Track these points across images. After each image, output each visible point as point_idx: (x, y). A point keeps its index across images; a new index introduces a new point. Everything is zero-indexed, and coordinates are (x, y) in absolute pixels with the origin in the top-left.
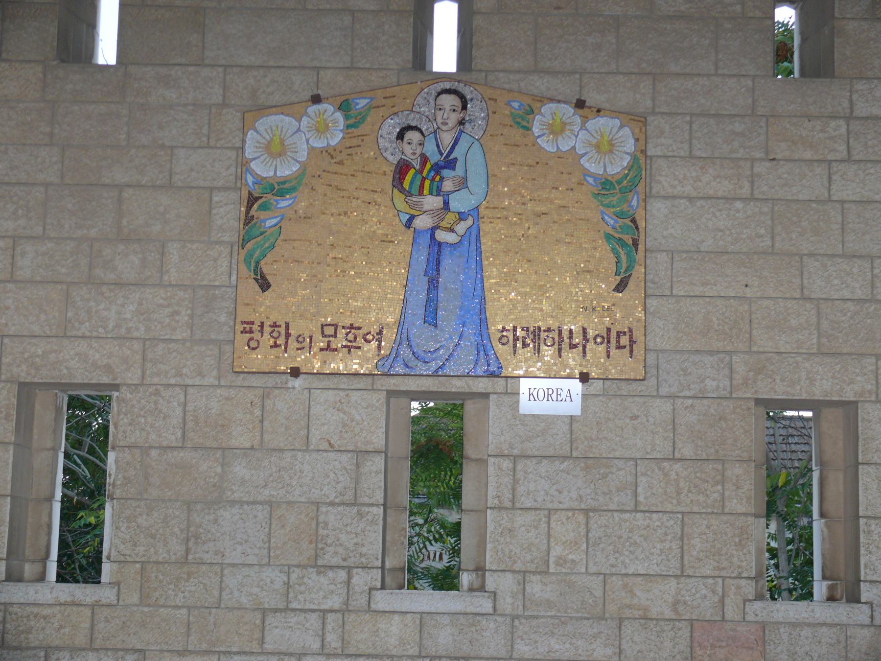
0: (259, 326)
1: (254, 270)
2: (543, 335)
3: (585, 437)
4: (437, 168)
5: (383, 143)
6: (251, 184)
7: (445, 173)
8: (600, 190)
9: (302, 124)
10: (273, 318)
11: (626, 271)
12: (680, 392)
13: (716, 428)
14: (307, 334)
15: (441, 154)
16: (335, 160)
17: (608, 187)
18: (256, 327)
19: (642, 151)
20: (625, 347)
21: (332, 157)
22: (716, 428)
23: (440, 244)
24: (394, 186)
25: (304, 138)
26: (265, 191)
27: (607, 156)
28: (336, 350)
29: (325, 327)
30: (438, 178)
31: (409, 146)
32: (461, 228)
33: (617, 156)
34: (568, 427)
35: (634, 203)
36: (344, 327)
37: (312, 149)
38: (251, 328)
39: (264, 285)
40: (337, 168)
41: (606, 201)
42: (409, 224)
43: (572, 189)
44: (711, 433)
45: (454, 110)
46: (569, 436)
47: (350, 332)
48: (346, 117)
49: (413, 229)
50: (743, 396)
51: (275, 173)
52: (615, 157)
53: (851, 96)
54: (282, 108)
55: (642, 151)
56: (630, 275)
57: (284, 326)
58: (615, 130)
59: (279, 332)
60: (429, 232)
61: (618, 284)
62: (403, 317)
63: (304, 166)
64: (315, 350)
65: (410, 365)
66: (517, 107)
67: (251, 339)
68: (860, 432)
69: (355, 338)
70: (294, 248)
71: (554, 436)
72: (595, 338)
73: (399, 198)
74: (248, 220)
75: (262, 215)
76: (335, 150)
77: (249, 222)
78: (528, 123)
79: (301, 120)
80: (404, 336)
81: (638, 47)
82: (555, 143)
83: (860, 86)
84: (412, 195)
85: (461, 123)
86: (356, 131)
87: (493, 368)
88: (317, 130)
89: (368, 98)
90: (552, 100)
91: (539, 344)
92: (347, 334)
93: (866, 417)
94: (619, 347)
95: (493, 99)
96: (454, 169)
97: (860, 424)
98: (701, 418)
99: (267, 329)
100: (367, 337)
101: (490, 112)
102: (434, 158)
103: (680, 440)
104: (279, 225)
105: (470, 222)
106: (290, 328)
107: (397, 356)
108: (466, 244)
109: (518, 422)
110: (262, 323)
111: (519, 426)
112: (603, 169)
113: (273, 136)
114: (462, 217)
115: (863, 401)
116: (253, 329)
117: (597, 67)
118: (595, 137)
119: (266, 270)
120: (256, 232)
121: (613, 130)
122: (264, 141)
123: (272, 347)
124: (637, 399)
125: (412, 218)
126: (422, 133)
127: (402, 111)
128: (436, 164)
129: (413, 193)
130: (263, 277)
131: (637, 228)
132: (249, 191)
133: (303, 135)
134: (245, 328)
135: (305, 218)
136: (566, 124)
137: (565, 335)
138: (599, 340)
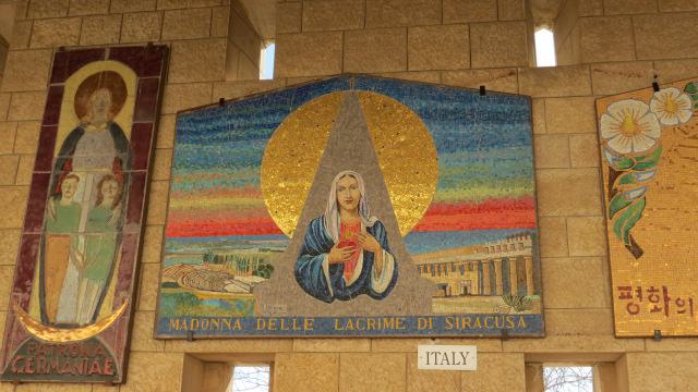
14: (686, 298)
18: (634, 294)
37: (664, 127)
39: (637, 252)
54: (629, 94)
57: (661, 290)
59: (657, 296)
63: (659, 142)
74: (612, 193)
75: (625, 187)
99: (645, 294)
120: (621, 203)
130: (634, 244)
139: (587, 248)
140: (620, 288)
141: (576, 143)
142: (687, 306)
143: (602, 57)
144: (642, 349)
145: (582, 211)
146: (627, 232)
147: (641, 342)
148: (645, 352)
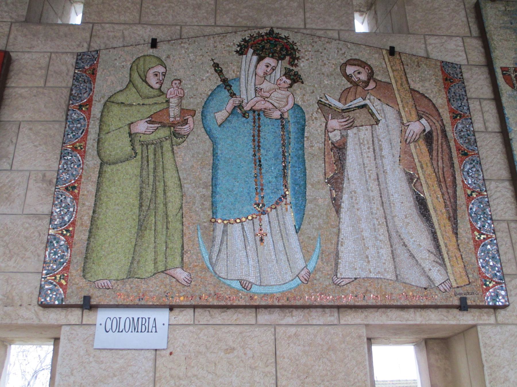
3: (172, 376)
12: (282, 320)
13: (325, 360)
22: (325, 360)
34: (151, 364)
44: (320, 366)
46: (151, 374)
50: (353, 323)
53: (426, 47)
68: (484, 359)
71: (135, 375)
81: (234, 7)
83: (431, 40)
93: (488, 342)
97: (483, 350)
98: (307, 348)
103: (283, 375)
109: (91, 359)
111: (93, 364)
115: (482, 324)
117: (197, 21)
124: (232, 328)
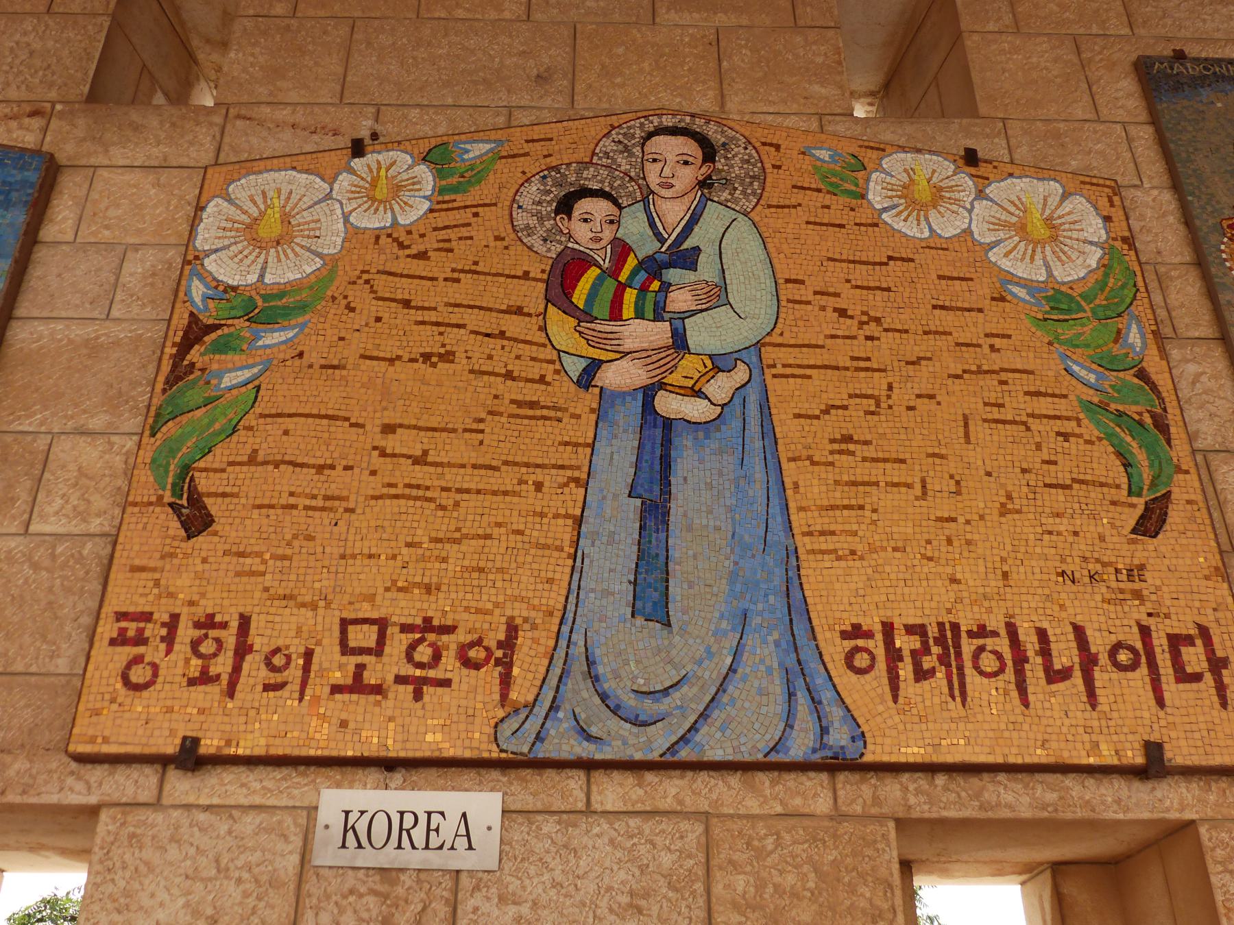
0: (164, 625)
1: (174, 485)
2: (968, 646)
4: (653, 267)
5: (521, 219)
6: (198, 299)
7: (673, 275)
8: (1046, 313)
9: (336, 186)
10: (207, 606)
11: (1153, 485)
14: (297, 648)
15: (662, 241)
16: (407, 252)
17: (1064, 306)
19: (1125, 240)
20: (1197, 677)
21: (401, 246)
23: (668, 423)
24: (548, 301)
25: (339, 212)
26: (233, 313)
27: (1048, 248)
28: (378, 690)
29: (351, 628)
30: (655, 285)
31: (584, 224)
32: (721, 387)
33: (1072, 248)
35: (1134, 337)
36: (406, 628)
37: (353, 233)
38: (141, 631)
40: (418, 267)
41: (1067, 332)
42: (587, 378)
43: (980, 310)
45: (686, 163)
47: (422, 640)
48: (439, 174)
49: (597, 391)
51: (262, 276)
52: (1066, 249)
55: (1125, 240)
56: (1167, 495)
57: (234, 624)
58: (1053, 201)
60: (640, 396)
61: (1142, 517)
62: (572, 599)
63: (331, 264)
64: (318, 688)
65: (594, 730)
66: (827, 159)
67: (138, 660)
69: (437, 657)
70: (286, 433)
72: (1113, 652)
73: (562, 329)
74: (179, 373)
76: (409, 232)
77: (181, 379)
78: (857, 185)
79: (335, 178)
80: (578, 650)
82: (923, 223)
84: (593, 319)
85: (705, 184)
86: (460, 200)
87: (839, 737)
88: (373, 199)
89: (495, 141)
90: (903, 149)
91: (961, 669)
92: (412, 647)
94: (1184, 676)
95: (771, 145)
96: (693, 266)
99: (185, 633)
100: (472, 653)
101: (768, 166)
102: (646, 246)
104: (256, 383)
105: (741, 374)
106: (252, 631)
107: (554, 707)
108: (736, 424)
110: (175, 617)
112: (1043, 271)
113: (267, 207)
114: (719, 364)
116: (147, 633)
118: (1012, 214)
119: (204, 483)
120: (194, 396)
121: (1050, 200)
122: (244, 218)
123: (192, 682)
125: (594, 366)
126: (615, 202)
127: (568, 165)
128: (651, 258)
129: (595, 313)
130: (196, 500)
131: (1154, 388)
132: (192, 314)
133: (337, 206)
134: (123, 631)
135: (323, 367)
136: (941, 189)
137: (1030, 643)
138: (1123, 657)
139: (83, 516)
140: (121, 616)
141: (135, 268)
142: (294, 673)
143: (262, 91)
144: (146, 796)
145: (97, 422)
146: (186, 469)
147: (147, 777)
148: (156, 804)
